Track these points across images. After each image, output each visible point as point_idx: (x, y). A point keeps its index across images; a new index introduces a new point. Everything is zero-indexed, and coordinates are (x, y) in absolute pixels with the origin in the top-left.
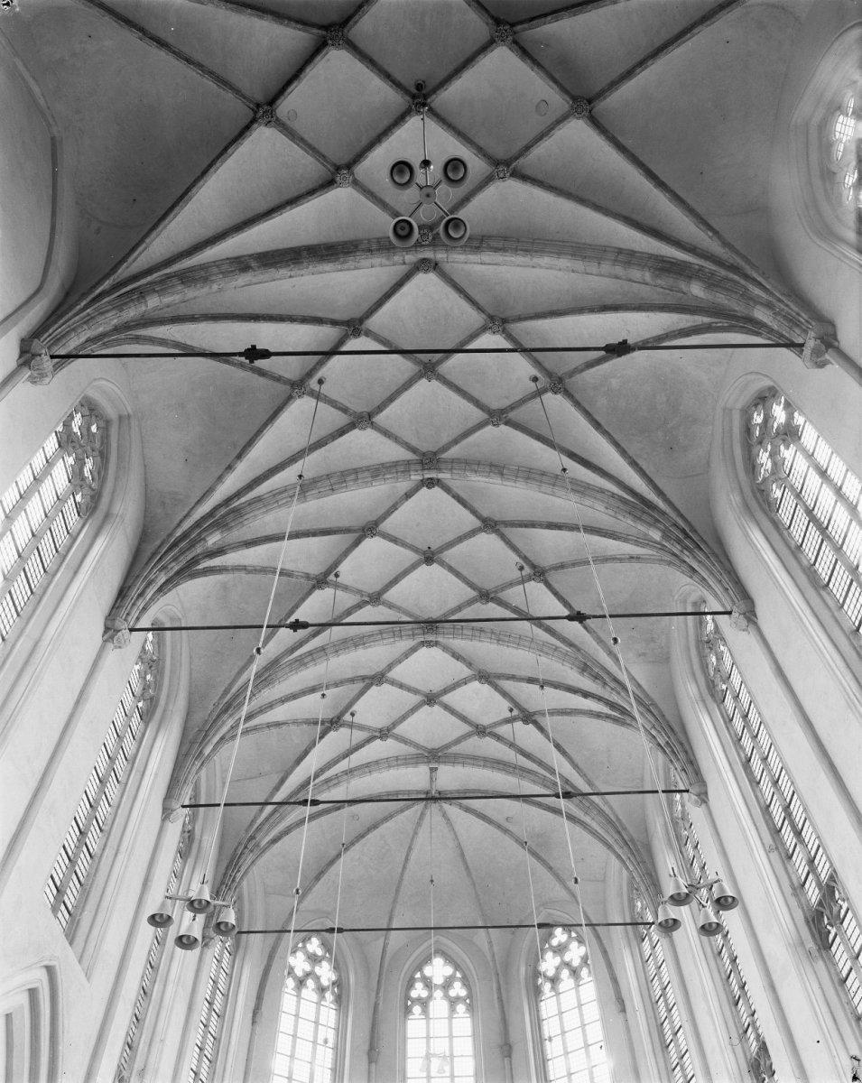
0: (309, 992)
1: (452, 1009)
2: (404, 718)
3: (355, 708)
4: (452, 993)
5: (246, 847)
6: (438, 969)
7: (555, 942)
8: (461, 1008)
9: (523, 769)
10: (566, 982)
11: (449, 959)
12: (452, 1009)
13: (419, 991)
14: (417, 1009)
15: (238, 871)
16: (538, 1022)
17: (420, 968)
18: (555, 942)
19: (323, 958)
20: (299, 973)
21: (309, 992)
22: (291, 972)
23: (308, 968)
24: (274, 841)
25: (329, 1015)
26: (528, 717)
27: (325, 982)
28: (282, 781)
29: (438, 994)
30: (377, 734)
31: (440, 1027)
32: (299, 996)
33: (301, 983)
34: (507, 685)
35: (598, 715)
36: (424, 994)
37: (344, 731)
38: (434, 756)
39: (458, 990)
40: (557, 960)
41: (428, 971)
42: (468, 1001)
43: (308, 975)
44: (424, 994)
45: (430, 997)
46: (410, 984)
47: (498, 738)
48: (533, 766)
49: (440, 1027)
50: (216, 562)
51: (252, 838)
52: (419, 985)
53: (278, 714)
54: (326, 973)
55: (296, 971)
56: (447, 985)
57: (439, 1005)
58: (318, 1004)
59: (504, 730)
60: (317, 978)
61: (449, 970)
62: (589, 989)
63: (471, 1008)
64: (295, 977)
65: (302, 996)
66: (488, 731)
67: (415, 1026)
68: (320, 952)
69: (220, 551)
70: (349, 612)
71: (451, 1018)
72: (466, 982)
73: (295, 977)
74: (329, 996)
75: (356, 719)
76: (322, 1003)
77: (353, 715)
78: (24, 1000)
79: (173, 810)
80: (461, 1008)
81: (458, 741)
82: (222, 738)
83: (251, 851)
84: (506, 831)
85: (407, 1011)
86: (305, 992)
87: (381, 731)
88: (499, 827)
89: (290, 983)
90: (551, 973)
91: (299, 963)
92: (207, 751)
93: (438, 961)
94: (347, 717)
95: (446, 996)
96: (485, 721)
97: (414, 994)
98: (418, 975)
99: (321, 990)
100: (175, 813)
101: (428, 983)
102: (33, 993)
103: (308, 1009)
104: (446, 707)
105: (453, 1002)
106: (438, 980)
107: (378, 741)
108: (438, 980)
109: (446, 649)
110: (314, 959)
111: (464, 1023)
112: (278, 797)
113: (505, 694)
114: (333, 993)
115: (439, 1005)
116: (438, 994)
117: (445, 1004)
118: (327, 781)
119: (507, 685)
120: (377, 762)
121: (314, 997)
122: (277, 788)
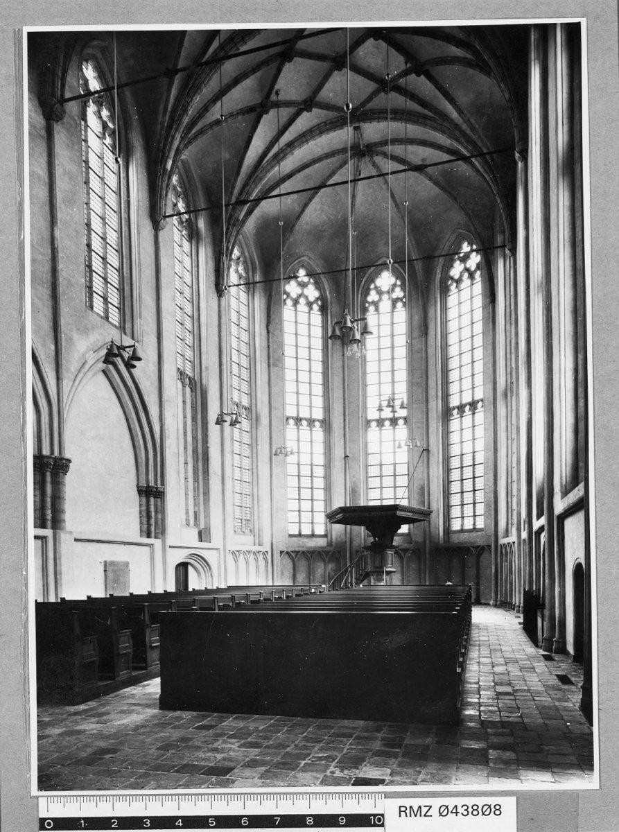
0: (302, 306)
1: (394, 306)
3: (277, 87)
8: (399, 305)
9: (425, 117)
10: (466, 281)
12: (394, 306)
13: (373, 296)
14: (372, 308)
17: (373, 281)
19: (309, 282)
20: (294, 296)
21: (302, 306)
22: (288, 295)
25: (317, 318)
29: (385, 297)
32: (296, 310)
33: (296, 302)
39: (398, 293)
45: (380, 300)
46: (367, 292)
53: (215, 113)
57: (385, 305)
62: (478, 287)
63: (404, 305)
64: (292, 299)
65: (298, 309)
68: (306, 279)
71: (393, 312)
72: (403, 287)
73: (292, 299)
74: (315, 307)
75: (282, 97)
76: (312, 312)
77: (277, 93)
80: (399, 305)
81: (370, 99)
89: (289, 302)
91: (292, 288)
97: (370, 299)
98: (372, 286)
99: (310, 304)
101: (380, 293)
103: (303, 317)
106: (385, 288)
108: (385, 288)
110: (303, 285)
111: (401, 314)
114: (318, 304)
115: (385, 305)
118: (276, 156)
121: (306, 309)
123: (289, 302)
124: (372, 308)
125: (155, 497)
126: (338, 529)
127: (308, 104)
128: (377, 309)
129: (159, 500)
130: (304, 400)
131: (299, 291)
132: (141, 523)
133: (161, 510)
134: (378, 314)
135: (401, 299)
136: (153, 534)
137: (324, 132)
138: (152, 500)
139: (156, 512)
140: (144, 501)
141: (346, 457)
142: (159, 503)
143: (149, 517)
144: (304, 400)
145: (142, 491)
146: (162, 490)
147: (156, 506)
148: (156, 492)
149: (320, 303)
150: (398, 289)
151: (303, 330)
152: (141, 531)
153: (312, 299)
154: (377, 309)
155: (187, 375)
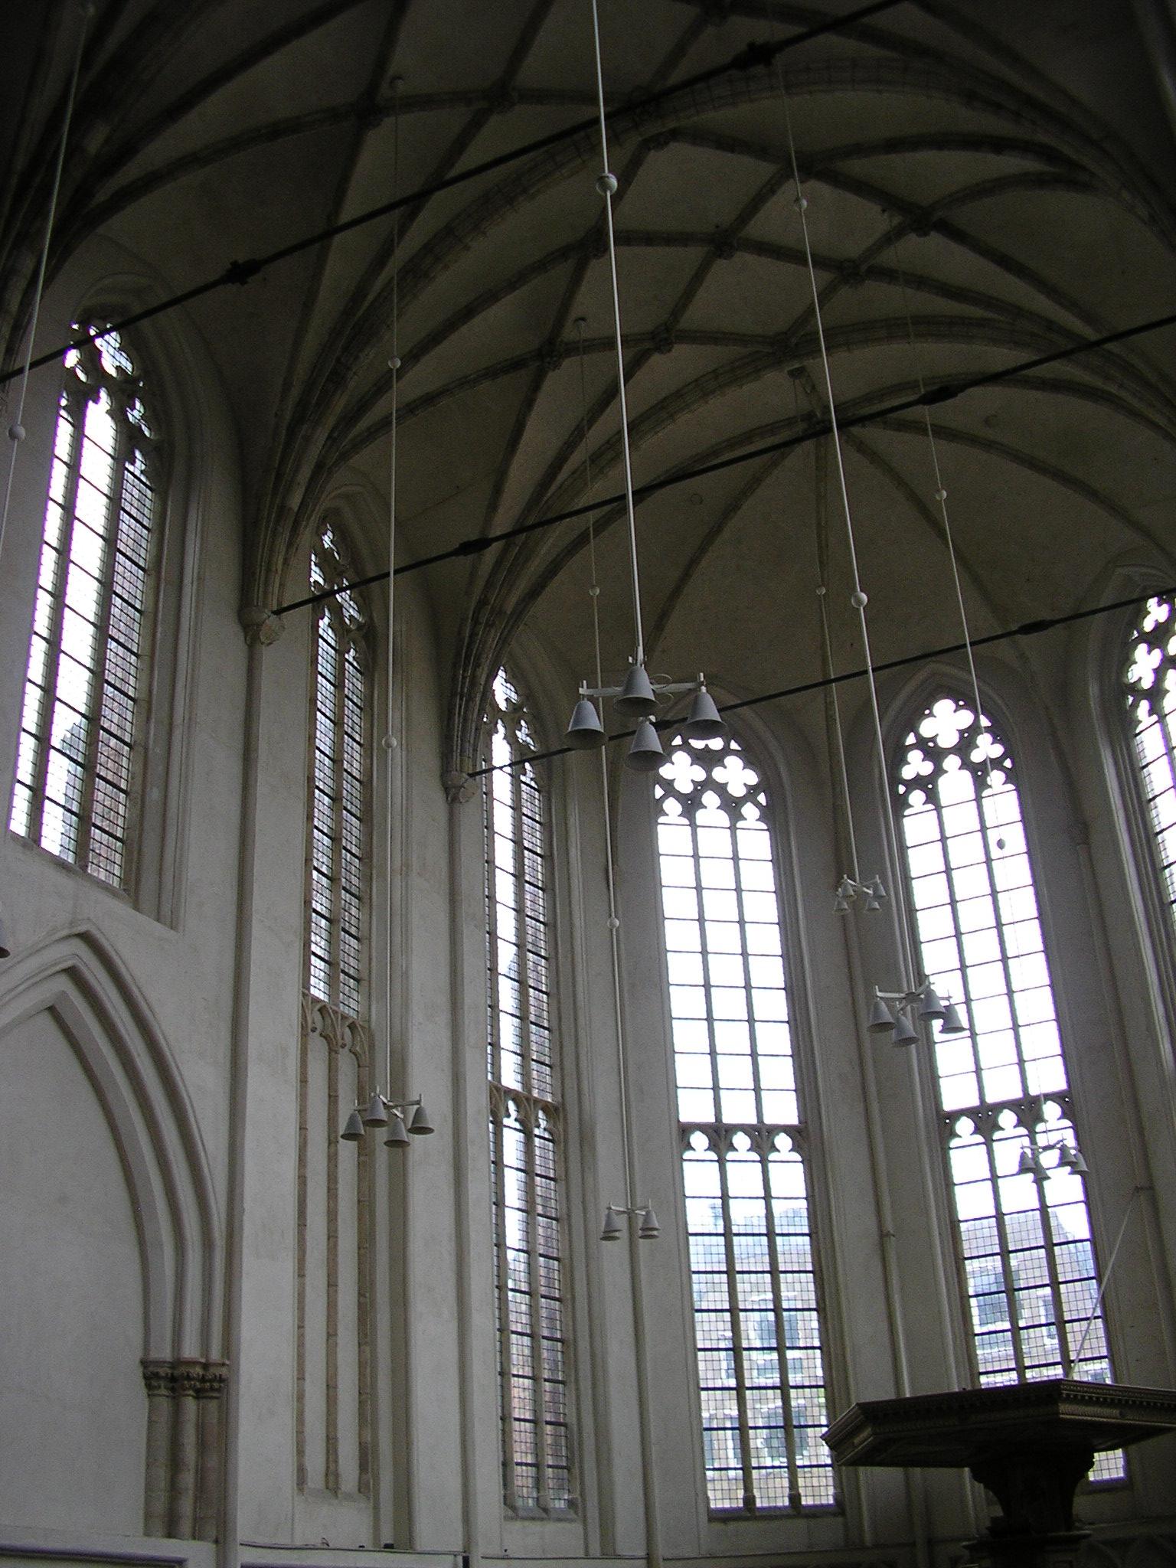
1: (980, 784)
2: (688, 295)
4: (976, 756)
5: (476, 621)
6: (945, 721)
7: (1148, 625)
8: (996, 778)
11: (963, 698)
12: (980, 784)
13: (916, 765)
14: (917, 797)
15: (477, 665)
16: (1132, 772)
18: (1148, 625)
19: (726, 751)
20: (685, 787)
22: (669, 786)
23: (700, 774)
24: (534, 593)
26: (920, 218)
27: (737, 790)
28: (498, 490)
29: (952, 762)
30: (647, 345)
31: (961, 817)
32: (693, 825)
33: (691, 804)
34: (857, 167)
35: (1039, 181)
36: (927, 768)
37: (569, 365)
38: (788, 347)
39: (987, 748)
40: (1157, 654)
41: (927, 728)
42: (1008, 763)
43: (700, 787)
44: (927, 768)
45: (939, 771)
46: (898, 758)
47: (889, 275)
48: (977, 312)
49: (961, 817)
50: (131, 171)
51: (482, 603)
52: (915, 757)
54: (737, 775)
55: (677, 786)
56: (966, 743)
57: (955, 782)
58: (733, 829)
59: (889, 257)
60: (721, 789)
61: (966, 718)
63: (1011, 777)
66: (864, 268)
67: (917, 824)
69: (125, 151)
70: (460, 145)
71: (978, 799)
72: (998, 734)
74: (750, 811)
76: (740, 824)
78: (64, 984)
79: (259, 625)
80: (996, 778)
82: (319, 467)
83: (489, 625)
84: (989, 445)
85: (901, 804)
86: (701, 816)
87: (653, 335)
88: (973, 440)
89: (672, 806)
90: (1146, 684)
92: (295, 501)
93: (944, 707)
94: (569, 334)
95: (966, 764)
96: (852, 249)
97: (907, 773)
98: (911, 739)
99: (732, 806)
100: (264, 628)
101: (934, 753)
102: (73, 973)
104: (764, 249)
105: (979, 774)
106: (948, 739)
107: (656, 359)
108: (948, 739)
109: (698, 137)
110: (708, 760)
111: (1004, 803)
112: (502, 523)
113: (861, 187)
114: (757, 804)
115: (955, 782)
116: (952, 762)
117: (966, 775)
119: (857, 167)
120: (678, 394)
121: (723, 819)
122: (493, 506)
123: (672, 806)
124: (917, 797)
125: (199, 1395)
126: (882, 1480)
127: (657, 339)
128: (932, 797)
129: (213, 1405)
130: (735, 1072)
131: (700, 774)
132: (149, 1488)
133: (218, 1439)
134: (938, 808)
135: (997, 763)
136: (186, 1526)
137: (713, 392)
138: (190, 1405)
139: (202, 1446)
140: (164, 1404)
141: (883, 1235)
142: (213, 1418)
143: (175, 1464)
144: (735, 1072)
145: (156, 1376)
146: (224, 1371)
147: (201, 1428)
148: (203, 1380)
149: (762, 798)
150: (984, 740)
151: (718, 874)
152: (148, 1516)
153: (737, 790)
154: (932, 797)
155: (344, 1017)
